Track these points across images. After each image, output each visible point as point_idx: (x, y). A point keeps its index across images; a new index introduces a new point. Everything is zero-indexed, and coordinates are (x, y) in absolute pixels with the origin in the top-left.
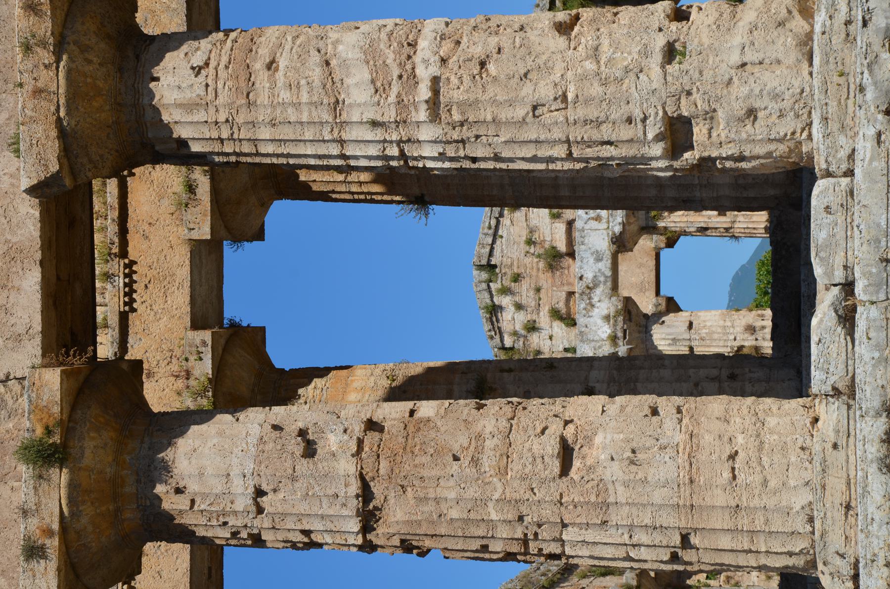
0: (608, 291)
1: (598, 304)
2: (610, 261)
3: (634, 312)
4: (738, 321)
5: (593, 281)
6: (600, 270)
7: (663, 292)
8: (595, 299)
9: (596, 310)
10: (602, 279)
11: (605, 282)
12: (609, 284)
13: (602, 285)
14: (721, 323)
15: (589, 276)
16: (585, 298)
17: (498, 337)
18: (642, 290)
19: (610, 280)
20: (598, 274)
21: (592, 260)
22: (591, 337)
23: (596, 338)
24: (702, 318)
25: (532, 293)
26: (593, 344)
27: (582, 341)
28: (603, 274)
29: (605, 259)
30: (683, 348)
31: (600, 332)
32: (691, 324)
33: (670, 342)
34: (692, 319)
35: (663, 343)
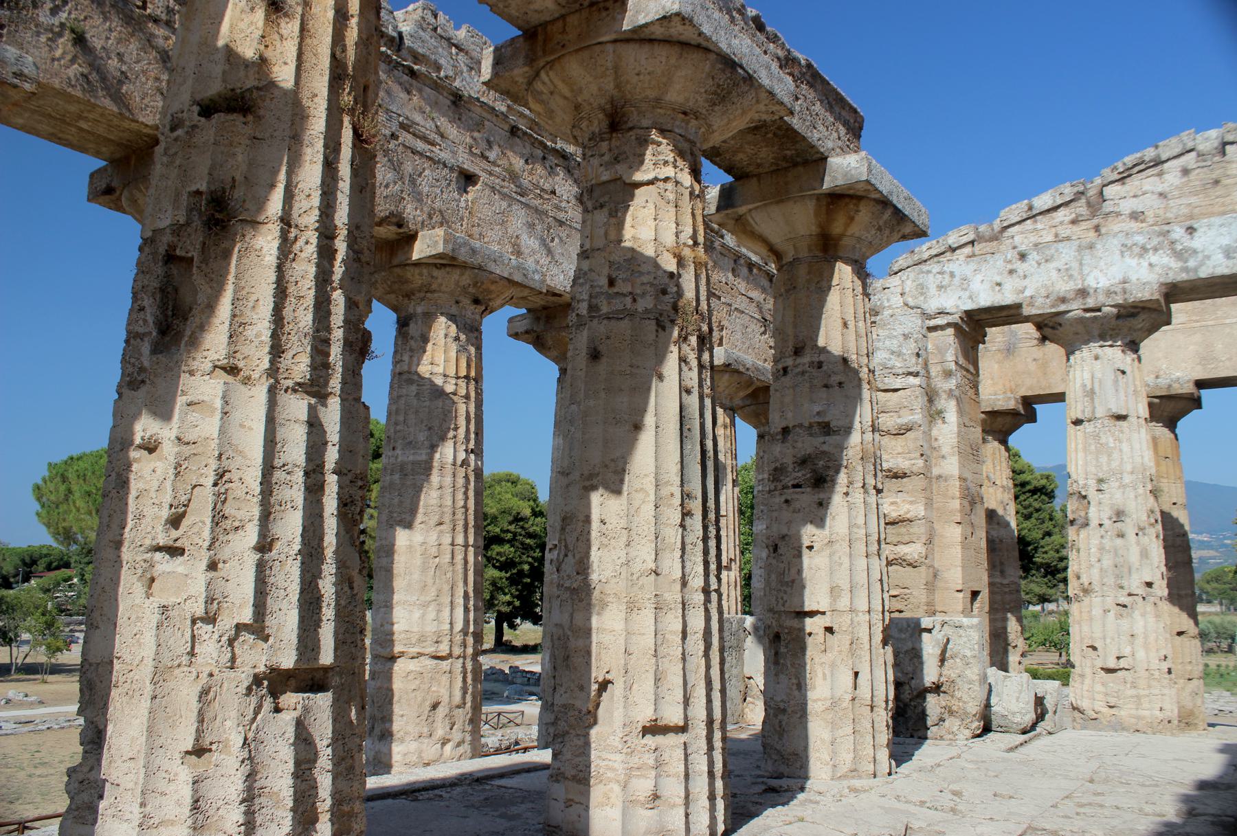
0: (1172, 277)
1: (1145, 264)
2: (1227, 271)
3: (1140, 322)
4: (1132, 495)
5: (1186, 250)
6: (1208, 257)
7: (1205, 394)
8: (1154, 258)
9: (1134, 262)
10: (1192, 263)
11: (1186, 270)
12: (1184, 276)
13: (1180, 264)
14: (1129, 468)
15: (1197, 242)
16: (1155, 241)
17: (1116, 176)
18: (1204, 360)
19: (1192, 276)
20: (1200, 256)
21: (1225, 241)
22: (1087, 259)
23: (1086, 270)
24: (1135, 435)
25: (1185, 211)
26: (1075, 265)
27: (1080, 248)
28: (1202, 264)
29: (1230, 263)
30: (1080, 407)
31: (1096, 273)
32: (1121, 418)
33: (1089, 387)
34: (1132, 419)
35: (1087, 376)
